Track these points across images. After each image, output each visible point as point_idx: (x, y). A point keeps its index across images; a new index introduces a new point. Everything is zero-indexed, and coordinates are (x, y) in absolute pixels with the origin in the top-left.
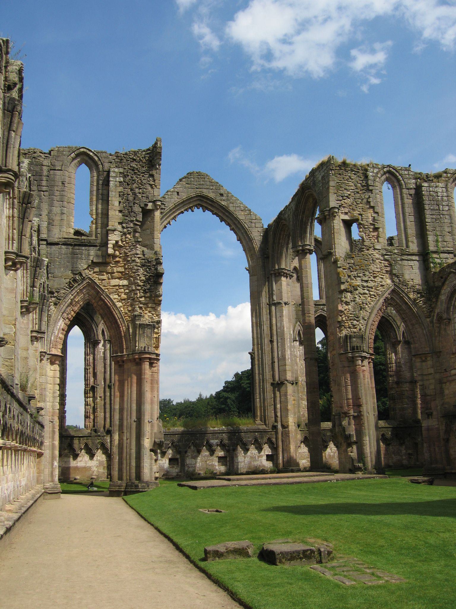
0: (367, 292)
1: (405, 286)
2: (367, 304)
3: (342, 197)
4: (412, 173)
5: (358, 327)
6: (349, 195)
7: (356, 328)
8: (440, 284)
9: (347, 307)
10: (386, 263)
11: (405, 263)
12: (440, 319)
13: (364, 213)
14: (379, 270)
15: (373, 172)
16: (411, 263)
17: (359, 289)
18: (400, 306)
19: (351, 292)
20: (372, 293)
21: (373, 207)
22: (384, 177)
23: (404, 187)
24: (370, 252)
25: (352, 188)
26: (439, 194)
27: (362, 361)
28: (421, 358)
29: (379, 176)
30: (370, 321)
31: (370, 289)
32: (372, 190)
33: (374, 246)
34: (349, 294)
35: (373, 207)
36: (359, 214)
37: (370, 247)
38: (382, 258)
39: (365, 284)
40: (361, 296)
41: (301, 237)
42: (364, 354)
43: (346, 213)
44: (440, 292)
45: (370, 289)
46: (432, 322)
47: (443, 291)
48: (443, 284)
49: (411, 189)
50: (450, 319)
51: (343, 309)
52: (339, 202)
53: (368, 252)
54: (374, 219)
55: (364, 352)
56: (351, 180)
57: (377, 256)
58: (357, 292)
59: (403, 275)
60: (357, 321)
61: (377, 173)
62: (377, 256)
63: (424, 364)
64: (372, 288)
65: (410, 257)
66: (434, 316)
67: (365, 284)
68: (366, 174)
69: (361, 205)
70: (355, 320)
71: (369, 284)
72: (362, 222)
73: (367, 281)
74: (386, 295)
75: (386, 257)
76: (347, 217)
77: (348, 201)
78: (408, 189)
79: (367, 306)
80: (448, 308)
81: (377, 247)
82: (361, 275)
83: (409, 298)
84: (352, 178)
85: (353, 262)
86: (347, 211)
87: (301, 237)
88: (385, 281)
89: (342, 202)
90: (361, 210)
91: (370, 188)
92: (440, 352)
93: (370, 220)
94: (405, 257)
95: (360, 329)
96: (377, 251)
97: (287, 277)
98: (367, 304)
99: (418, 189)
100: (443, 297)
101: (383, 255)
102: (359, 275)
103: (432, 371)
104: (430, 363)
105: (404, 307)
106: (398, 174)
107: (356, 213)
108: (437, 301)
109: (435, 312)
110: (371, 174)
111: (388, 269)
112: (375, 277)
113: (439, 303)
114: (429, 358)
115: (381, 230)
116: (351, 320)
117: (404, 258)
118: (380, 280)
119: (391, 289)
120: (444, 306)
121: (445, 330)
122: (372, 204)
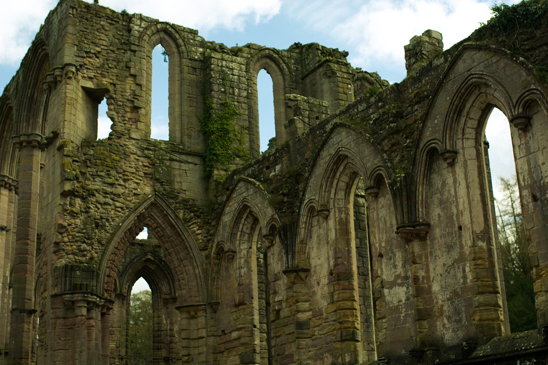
0: (111, 202)
1: (173, 198)
2: (107, 220)
3: (86, 52)
4: (198, 39)
5: (89, 255)
6: (99, 52)
7: (85, 256)
8: (225, 198)
9: (73, 221)
10: (146, 162)
11: (176, 165)
12: (220, 251)
13: (119, 82)
14: (134, 170)
15: (140, 26)
16: (184, 166)
17: (97, 195)
18: (163, 230)
19: (83, 198)
20: (118, 204)
21: (134, 76)
22: (157, 37)
23: (185, 55)
24: (122, 143)
25: (104, 43)
26: (236, 72)
27: (89, 310)
28: (189, 312)
29: (148, 32)
30: (111, 248)
31: (116, 198)
32: (135, 51)
33: (129, 134)
34: (78, 201)
35: (134, 76)
36: (111, 84)
37: (123, 135)
38: (139, 153)
39: (109, 189)
40: (99, 206)
41: (28, 122)
42: (94, 299)
43: (91, 78)
44: (223, 209)
45: (116, 198)
46: (208, 257)
47: (227, 209)
48: (228, 199)
49: (196, 60)
50: (235, 252)
51: (65, 224)
52: (78, 59)
53: (118, 141)
54: (134, 94)
55: (92, 294)
56: (104, 32)
57: (133, 149)
58: (93, 199)
59: (170, 183)
60: (89, 245)
61: (146, 28)
62: (133, 149)
63: (193, 322)
64: (119, 196)
65: (184, 157)
66: (212, 246)
67: (109, 189)
68: (129, 26)
69: (115, 71)
70: (84, 242)
71: (113, 190)
72: (114, 96)
73: (112, 185)
74: (141, 209)
75: (146, 152)
76: (89, 85)
77: (97, 62)
78: (191, 59)
79: (107, 224)
80: (233, 235)
81: (134, 135)
82: (103, 174)
83: (177, 217)
84: (107, 28)
85: (92, 152)
86: (92, 74)
87: (28, 122)
88: (142, 189)
89: (86, 61)
90: (114, 78)
91: (133, 47)
92: (218, 304)
93: (128, 94)
94: (176, 157)
95: (92, 258)
96: (134, 142)
97: (10, 190)
98: (107, 220)
99: (206, 62)
100: (227, 219)
101: (142, 149)
102: (99, 173)
103: (203, 333)
104: (202, 320)
105: (168, 231)
106: (177, 36)
107: (105, 81)
108: (218, 224)
109: (214, 241)
110: (136, 28)
111: (150, 171)
112: (125, 181)
113: (221, 228)
114: (200, 313)
115: (143, 111)
116: (77, 241)
117: (175, 158)
118: (134, 186)
119: (149, 202)
120: (228, 230)
121: (227, 269)
122: (133, 71)
